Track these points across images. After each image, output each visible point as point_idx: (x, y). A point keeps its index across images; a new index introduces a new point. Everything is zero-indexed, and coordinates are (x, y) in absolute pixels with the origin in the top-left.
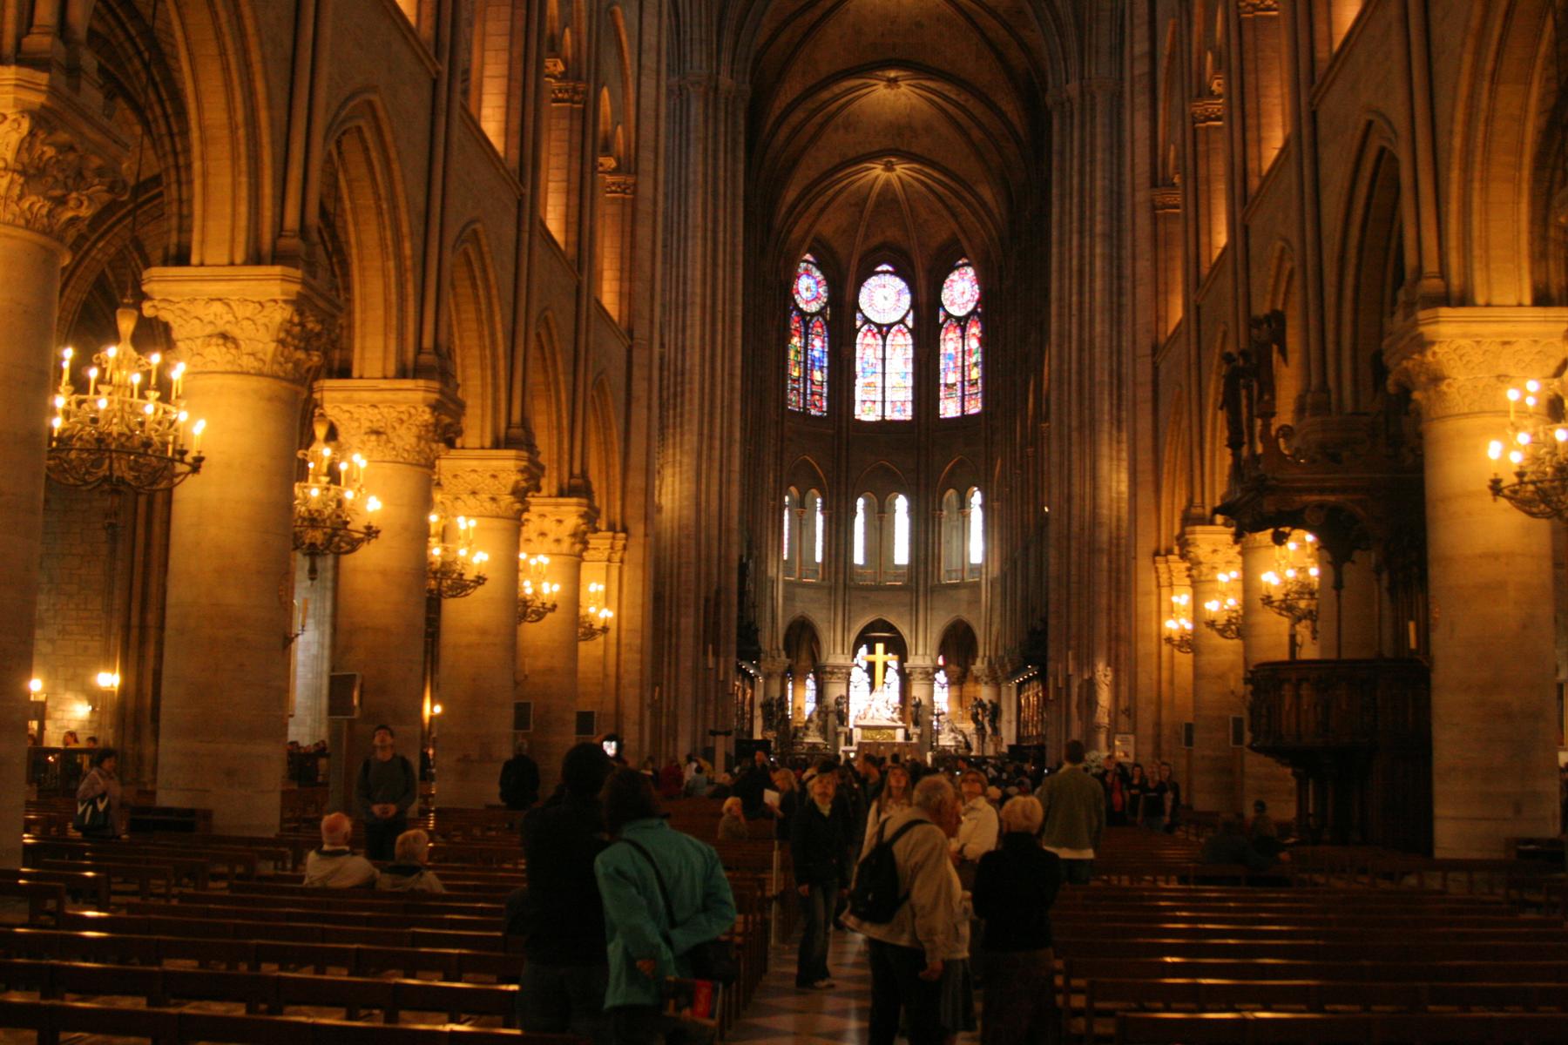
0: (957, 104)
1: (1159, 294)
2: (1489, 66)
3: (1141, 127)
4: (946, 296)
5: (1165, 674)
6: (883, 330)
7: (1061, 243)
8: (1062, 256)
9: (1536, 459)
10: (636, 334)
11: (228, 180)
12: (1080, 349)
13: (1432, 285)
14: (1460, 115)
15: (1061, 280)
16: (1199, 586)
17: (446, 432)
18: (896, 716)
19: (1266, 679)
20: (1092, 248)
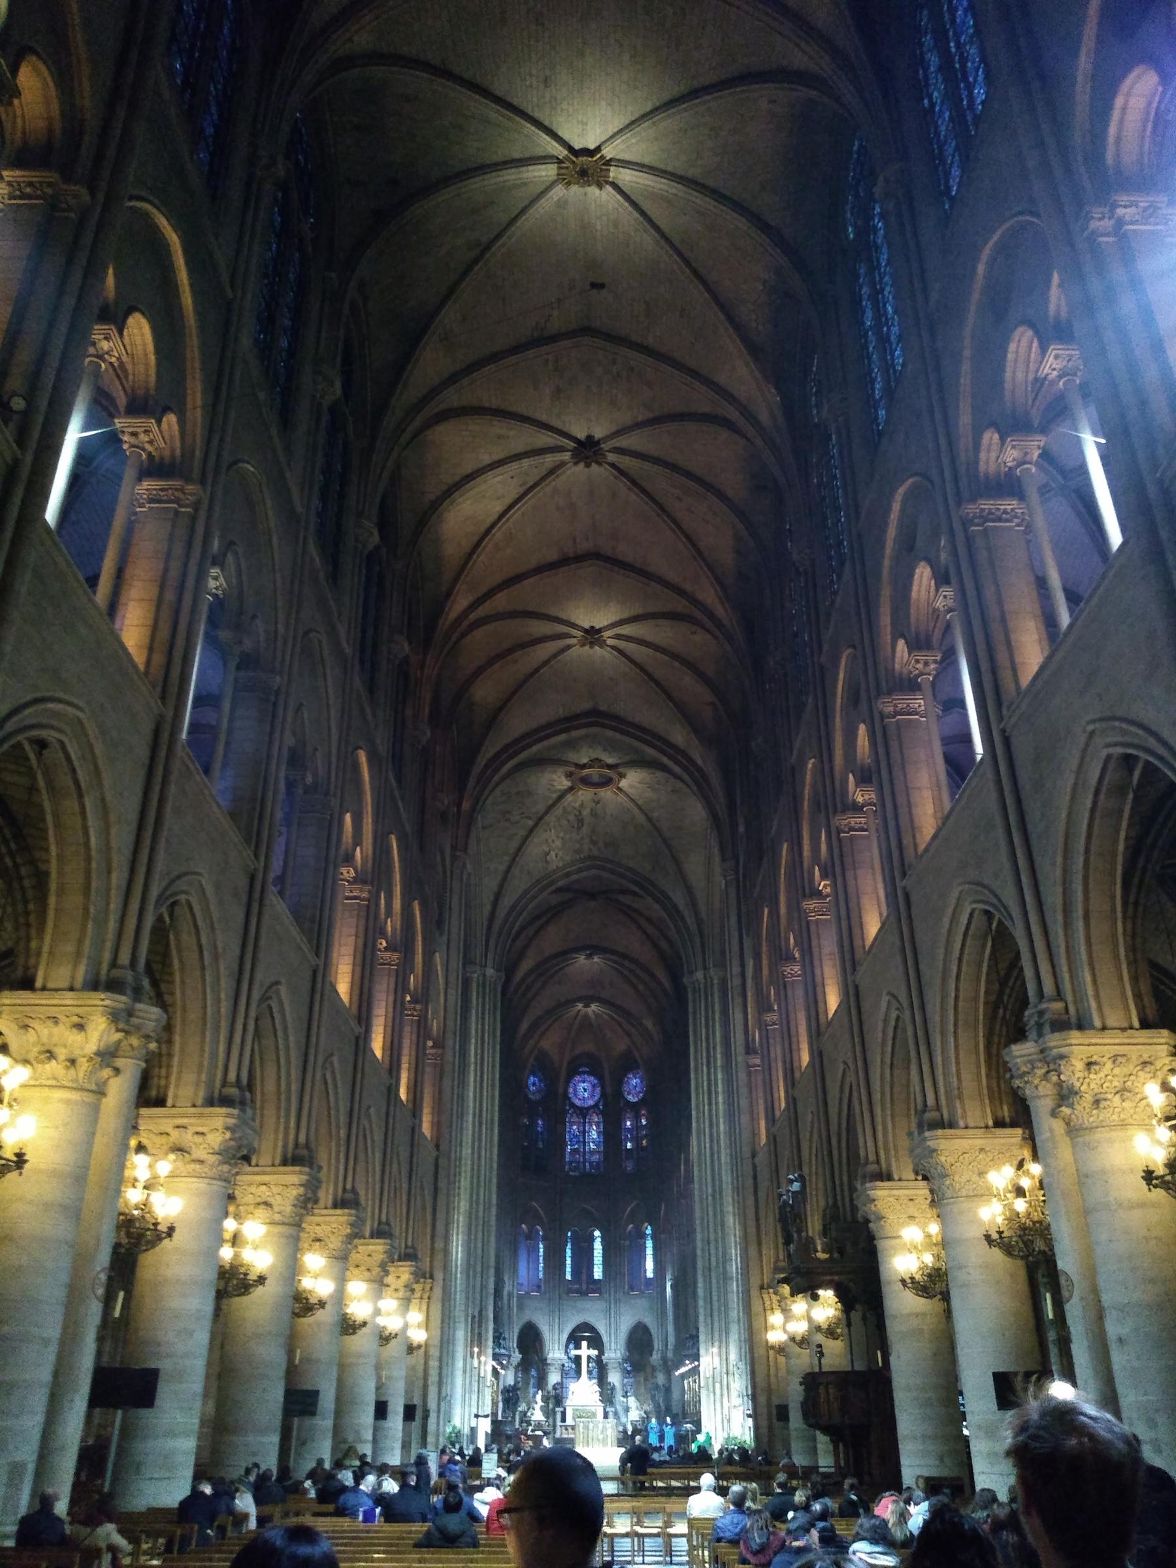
0: (631, 971)
1: (753, 1119)
2: (888, 1061)
3: (739, 1016)
4: (625, 1088)
5: (772, 1372)
6: (583, 1112)
7: (696, 1070)
8: (698, 1079)
9: (921, 1269)
10: (441, 1148)
11: (274, 1120)
12: (711, 1141)
13: (872, 1168)
14: (878, 1083)
15: (697, 1095)
16: (785, 1311)
17: (355, 1235)
18: (597, 1397)
19: (812, 1381)
20: (716, 1074)
